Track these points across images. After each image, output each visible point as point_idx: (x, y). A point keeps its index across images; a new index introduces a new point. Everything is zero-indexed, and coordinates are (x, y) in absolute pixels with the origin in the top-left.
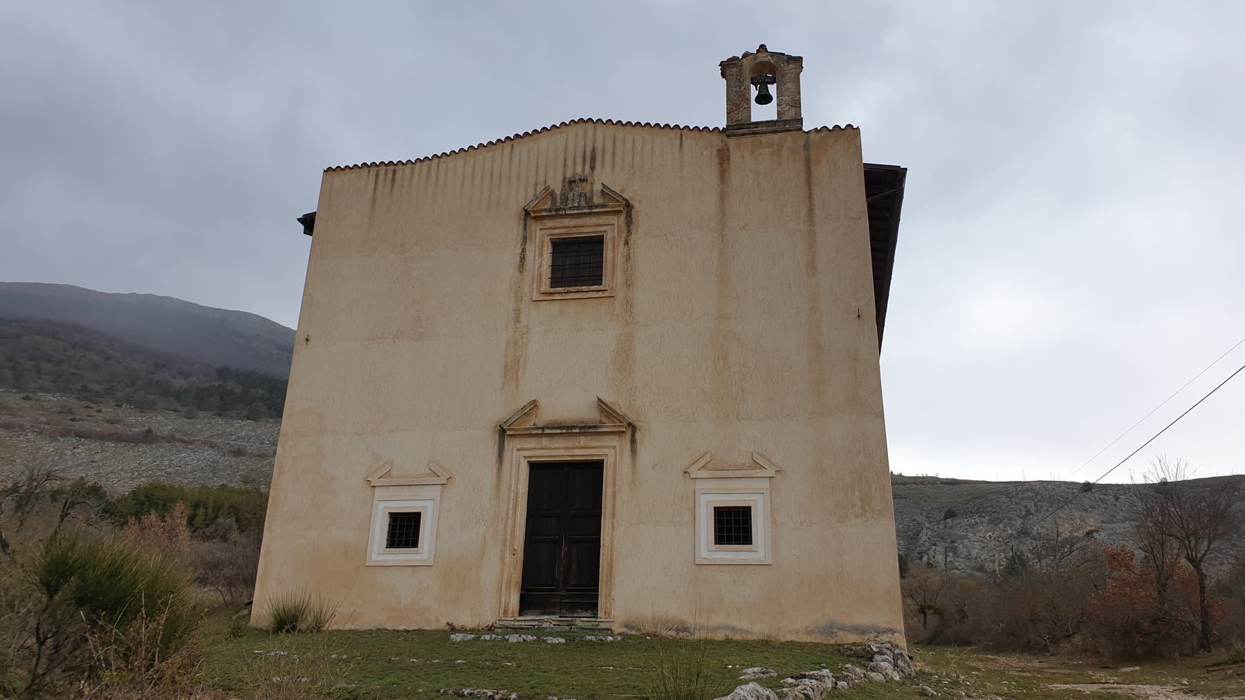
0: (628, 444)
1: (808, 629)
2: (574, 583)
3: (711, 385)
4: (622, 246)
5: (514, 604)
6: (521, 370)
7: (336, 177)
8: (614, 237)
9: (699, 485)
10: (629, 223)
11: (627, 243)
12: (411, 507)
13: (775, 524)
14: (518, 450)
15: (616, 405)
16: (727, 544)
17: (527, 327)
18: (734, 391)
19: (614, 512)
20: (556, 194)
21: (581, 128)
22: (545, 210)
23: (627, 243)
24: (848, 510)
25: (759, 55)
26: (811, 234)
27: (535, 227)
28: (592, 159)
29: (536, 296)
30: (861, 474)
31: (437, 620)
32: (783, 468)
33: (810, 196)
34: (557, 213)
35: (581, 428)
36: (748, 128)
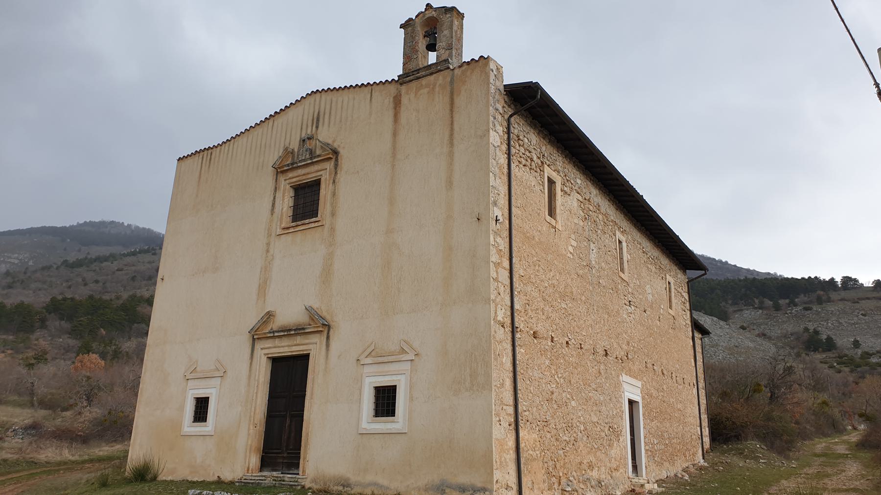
0: (325, 339)
1: (427, 486)
2: (291, 448)
3: (379, 288)
4: (331, 185)
5: (253, 464)
6: (268, 287)
7: (183, 163)
8: (326, 178)
9: (367, 369)
10: (336, 166)
11: (334, 182)
12: (204, 393)
13: (411, 399)
14: (262, 349)
15: (320, 310)
17: (273, 256)
18: (393, 291)
19: (312, 394)
20: (295, 152)
21: (312, 99)
22: (288, 165)
23: (334, 182)
24: (461, 385)
25: (427, 12)
26: (451, 155)
27: (282, 178)
28: (317, 121)
29: (279, 231)
30: (472, 354)
31: (214, 475)
32: (420, 353)
33: (452, 123)
34: (293, 167)
35: (295, 330)
36: (413, 75)
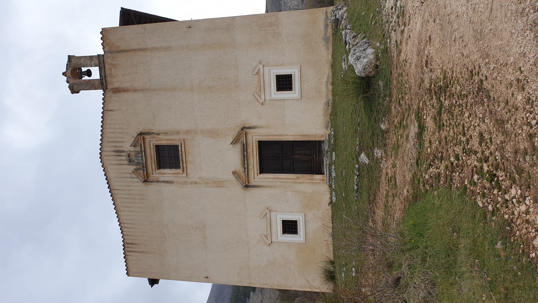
1: (326, 49)
2: (310, 152)
4: (160, 136)
5: (320, 177)
6: (219, 180)
9: (268, 98)
10: (149, 133)
11: (158, 134)
13: (283, 64)
15: (234, 136)
16: (292, 78)
17: (199, 178)
18: (226, 83)
20: (136, 168)
21: (104, 158)
23: (158, 134)
24: (276, 32)
25: (67, 75)
26: (152, 49)
27: (152, 177)
28: (119, 152)
29: (185, 175)
31: (327, 210)
33: (134, 50)
34: (145, 167)
35: (244, 151)
36: (103, 79)
